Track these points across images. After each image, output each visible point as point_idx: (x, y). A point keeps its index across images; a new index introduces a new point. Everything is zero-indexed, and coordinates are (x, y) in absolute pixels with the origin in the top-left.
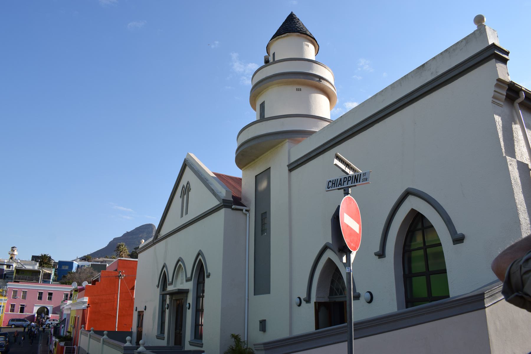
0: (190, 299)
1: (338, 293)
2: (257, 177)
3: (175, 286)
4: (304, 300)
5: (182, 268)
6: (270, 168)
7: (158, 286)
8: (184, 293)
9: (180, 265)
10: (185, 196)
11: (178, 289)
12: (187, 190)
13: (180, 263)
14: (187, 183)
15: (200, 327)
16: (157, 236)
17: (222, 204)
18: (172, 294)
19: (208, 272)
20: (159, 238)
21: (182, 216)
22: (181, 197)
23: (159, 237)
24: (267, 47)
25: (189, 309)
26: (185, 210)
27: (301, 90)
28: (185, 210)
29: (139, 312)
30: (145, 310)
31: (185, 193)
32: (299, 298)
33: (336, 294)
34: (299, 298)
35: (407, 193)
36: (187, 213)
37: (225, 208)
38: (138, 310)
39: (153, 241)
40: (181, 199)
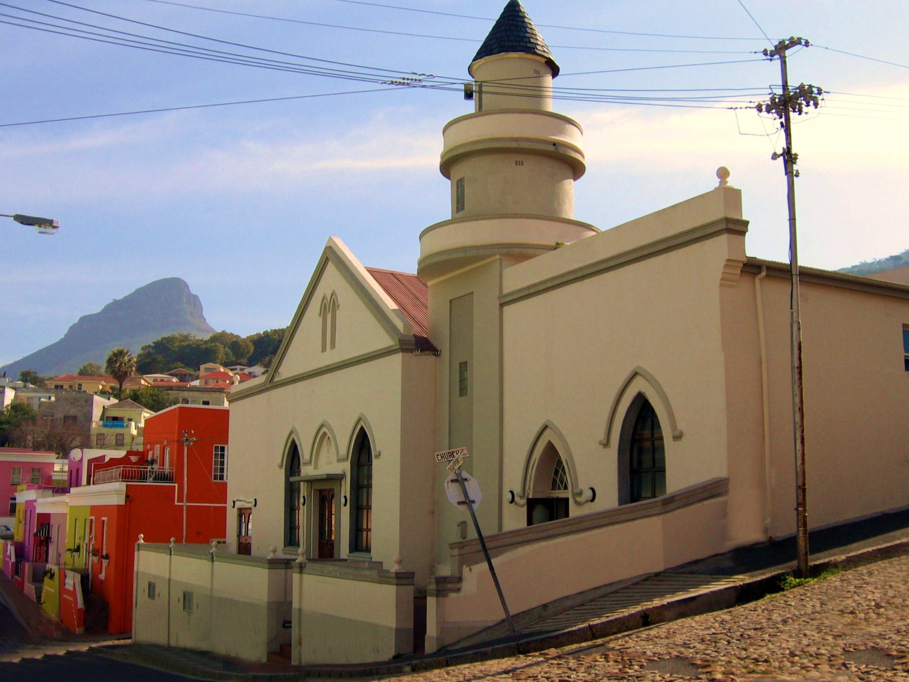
0: (346, 489)
1: (562, 486)
2: (453, 302)
3: (316, 468)
4: (518, 496)
5: (329, 438)
6: (472, 293)
7: (281, 467)
8: (337, 479)
9: (325, 434)
10: (329, 316)
11: (327, 475)
12: (330, 307)
13: (324, 429)
14: (332, 294)
15: (365, 533)
16: (273, 377)
17: (398, 347)
18: (311, 482)
19: (378, 449)
20: (277, 382)
21: (324, 349)
22: (320, 314)
23: (276, 379)
24: (469, 68)
25: (345, 505)
26: (329, 339)
27: (522, 164)
28: (329, 339)
29: (240, 510)
30: (255, 506)
31: (329, 310)
32: (512, 492)
33: (559, 489)
34: (512, 492)
35: (635, 375)
36: (333, 346)
37: (402, 352)
38: (238, 505)
39: (265, 383)
40: (321, 318)
